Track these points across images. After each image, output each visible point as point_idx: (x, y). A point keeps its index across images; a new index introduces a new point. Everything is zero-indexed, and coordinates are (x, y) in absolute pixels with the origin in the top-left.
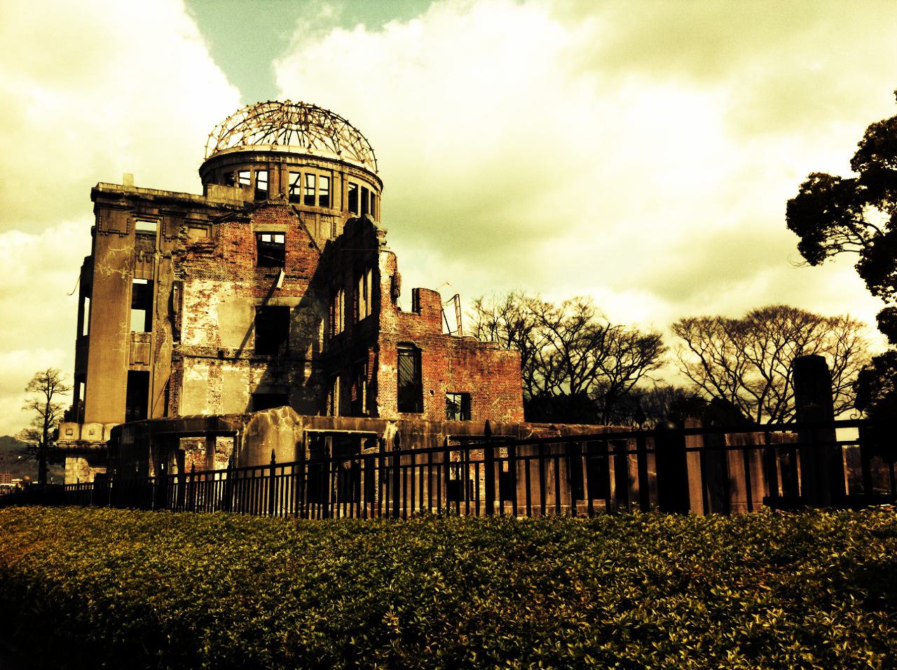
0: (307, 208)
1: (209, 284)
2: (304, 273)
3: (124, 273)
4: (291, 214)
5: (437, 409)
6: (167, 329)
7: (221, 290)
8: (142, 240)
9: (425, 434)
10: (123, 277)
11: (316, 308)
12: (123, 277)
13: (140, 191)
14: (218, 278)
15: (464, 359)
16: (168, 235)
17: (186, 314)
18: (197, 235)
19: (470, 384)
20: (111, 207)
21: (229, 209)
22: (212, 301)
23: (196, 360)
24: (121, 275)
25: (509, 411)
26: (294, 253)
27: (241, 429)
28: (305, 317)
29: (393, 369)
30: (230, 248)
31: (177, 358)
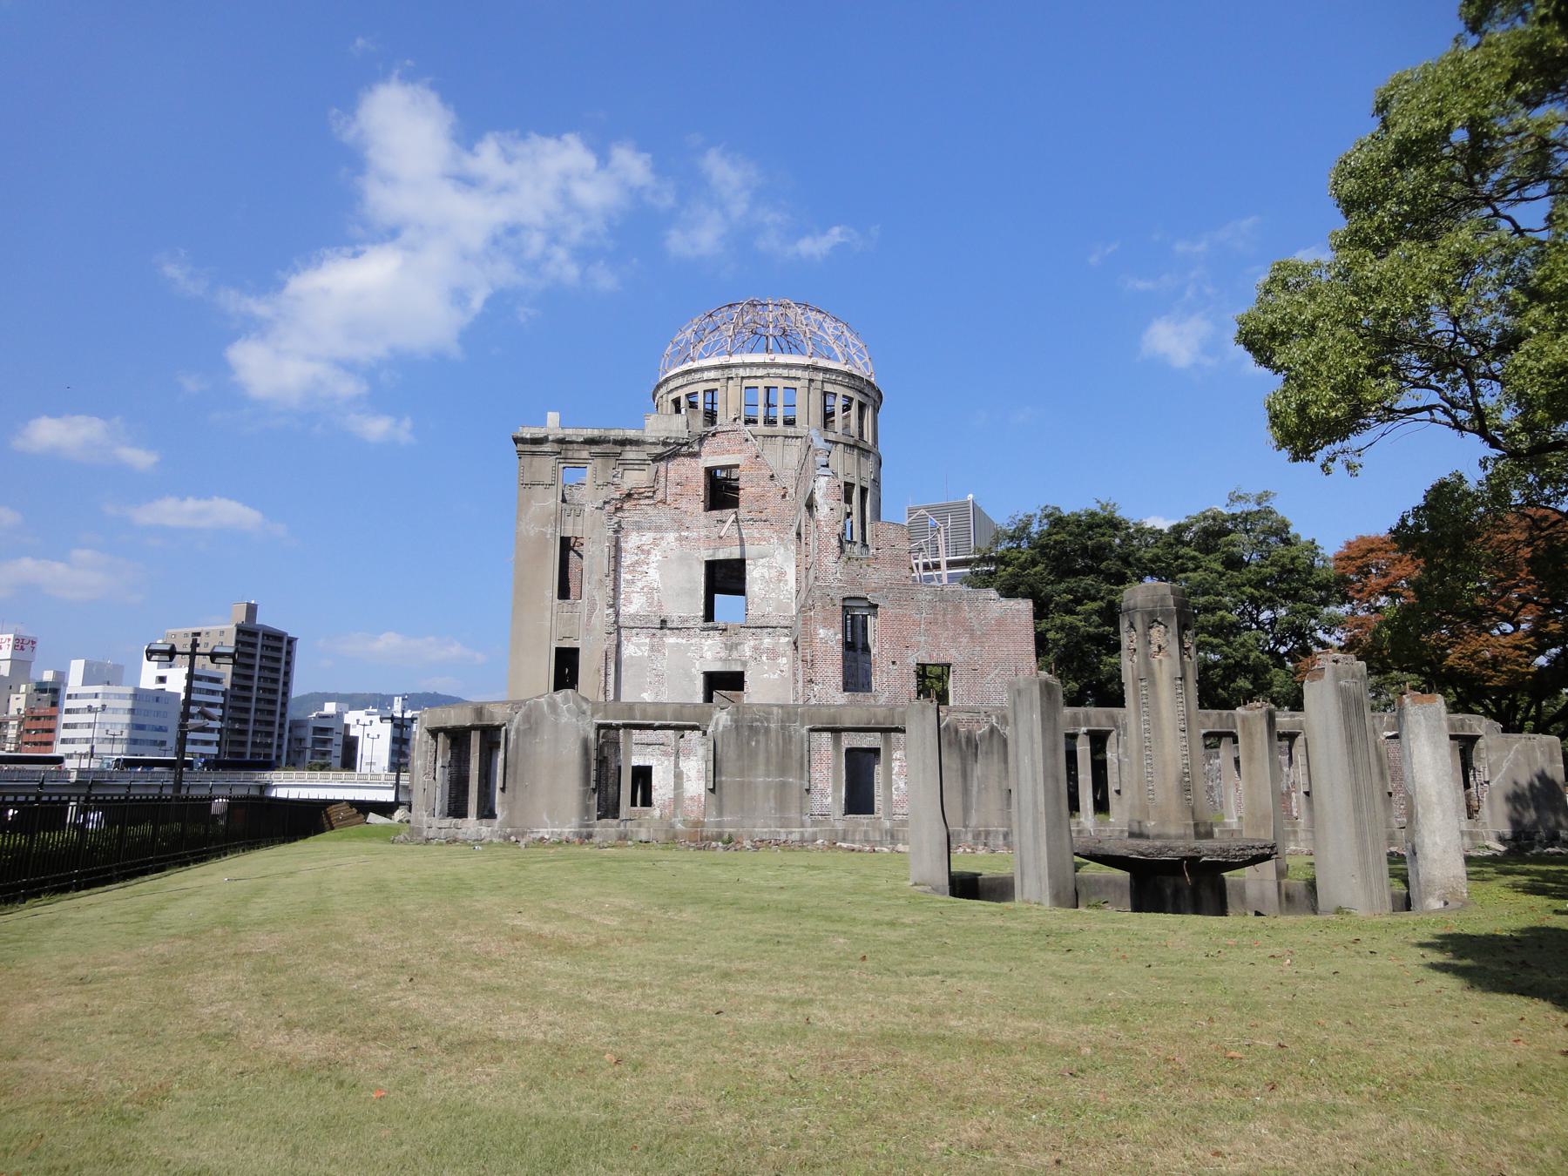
0: (768, 430)
1: (648, 537)
4: (747, 440)
5: (902, 686)
6: (602, 597)
7: (664, 544)
9: (772, 725)
10: (548, 536)
11: (779, 557)
12: (548, 536)
14: (659, 529)
15: (944, 615)
17: (625, 576)
18: (635, 479)
19: (953, 652)
20: (533, 454)
21: (670, 444)
22: (652, 557)
23: (634, 631)
24: (546, 534)
27: (510, 721)
28: (766, 570)
29: (836, 634)
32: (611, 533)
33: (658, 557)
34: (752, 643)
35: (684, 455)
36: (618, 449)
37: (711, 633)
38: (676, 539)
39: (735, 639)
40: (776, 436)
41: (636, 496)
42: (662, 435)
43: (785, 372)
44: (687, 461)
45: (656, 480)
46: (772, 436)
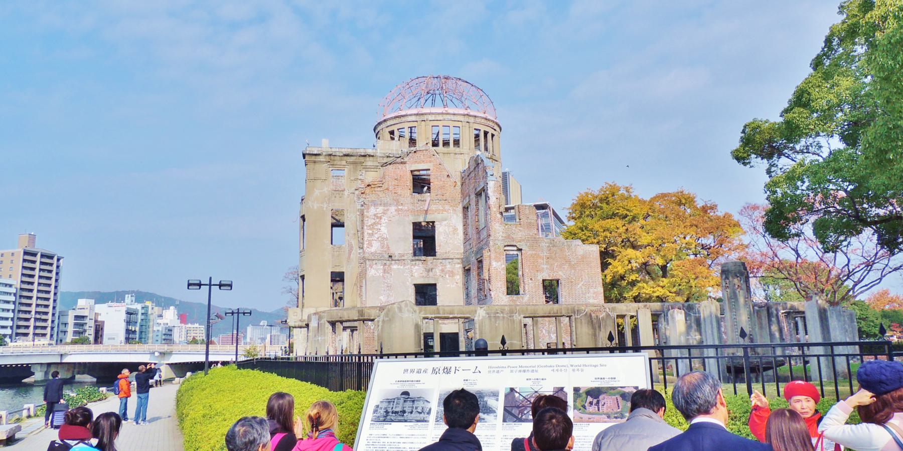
1: (380, 209)
2: (444, 197)
3: (325, 206)
7: (389, 213)
8: (340, 180)
10: (325, 209)
13: (333, 150)
14: (385, 205)
16: (352, 178)
17: (367, 231)
20: (315, 162)
22: (383, 221)
23: (374, 262)
25: (591, 290)
26: (438, 183)
30: (394, 183)
31: (364, 260)
32: (359, 207)
33: (386, 221)
34: (440, 268)
35: (398, 163)
36: (362, 159)
37: (417, 262)
38: (396, 210)
39: (430, 266)
40: (450, 154)
41: (373, 186)
42: (388, 152)
43: (456, 118)
44: (400, 166)
45: (384, 177)
46: (448, 153)
